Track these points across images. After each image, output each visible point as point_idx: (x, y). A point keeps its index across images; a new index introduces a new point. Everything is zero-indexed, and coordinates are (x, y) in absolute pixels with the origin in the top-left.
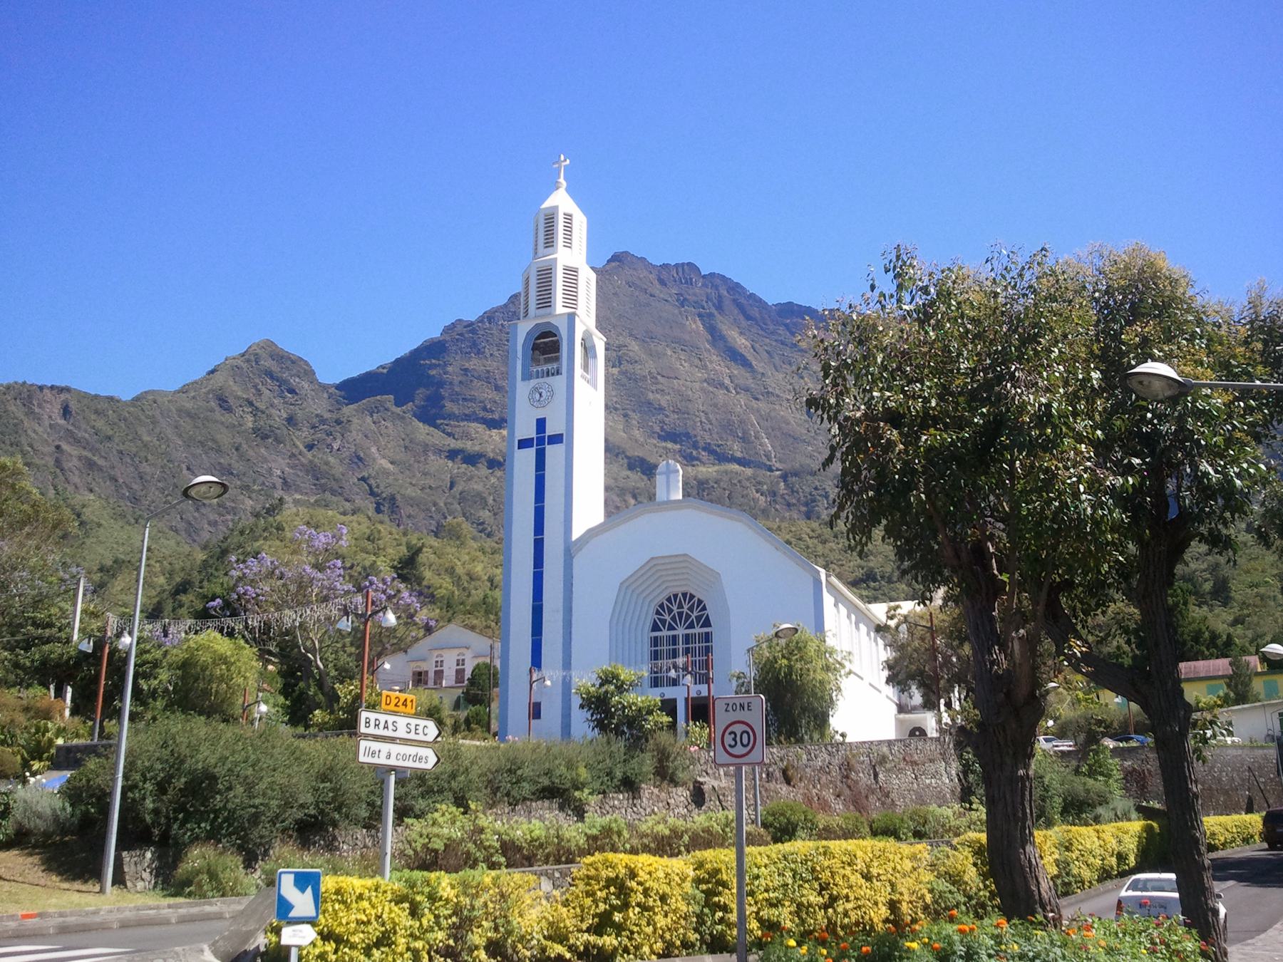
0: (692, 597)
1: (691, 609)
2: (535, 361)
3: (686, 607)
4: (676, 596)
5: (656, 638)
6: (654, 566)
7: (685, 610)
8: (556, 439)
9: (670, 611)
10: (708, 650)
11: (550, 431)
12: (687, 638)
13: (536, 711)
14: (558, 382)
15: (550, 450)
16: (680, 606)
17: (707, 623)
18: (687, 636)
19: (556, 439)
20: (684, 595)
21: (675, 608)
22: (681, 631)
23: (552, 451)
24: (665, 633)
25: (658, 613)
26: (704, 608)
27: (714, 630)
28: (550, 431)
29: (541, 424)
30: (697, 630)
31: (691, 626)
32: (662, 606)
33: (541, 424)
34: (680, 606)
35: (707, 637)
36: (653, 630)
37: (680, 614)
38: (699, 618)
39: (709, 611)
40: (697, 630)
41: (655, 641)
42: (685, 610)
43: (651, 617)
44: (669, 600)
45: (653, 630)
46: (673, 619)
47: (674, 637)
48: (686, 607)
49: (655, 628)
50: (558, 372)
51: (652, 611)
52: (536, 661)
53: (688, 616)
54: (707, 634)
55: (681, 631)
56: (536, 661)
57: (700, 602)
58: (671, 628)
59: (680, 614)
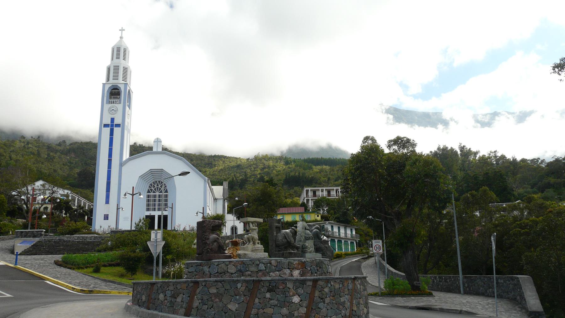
0: (162, 183)
2: (110, 98)
4: (156, 182)
6: (152, 172)
7: (159, 186)
8: (118, 125)
9: (154, 187)
11: (116, 122)
12: (159, 196)
13: (106, 217)
14: (120, 107)
15: (116, 129)
16: (158, 185)
17: (166, 191)
19: (118, 125)
20: (159, 182)
22: (157, 194)
23: (117, 130)
24: (152, 194)
25: (150, 187)
26: (166, 187)
28: (116, 122)
29: (112, 120)
31: (161, 192)
32: (151, 185)
33: (112, 120)
34: (158, 185)
35: (166, 196)
41: (148, 196)
42: (159, 186)
43: (148, 188)
44: (154, 183)
46: (155, 189)
49: (149, 192)
50: (120, 103)
51: (148, 186)
52: (107, 202)
53: (160, 189)
55: (157, 194)
56: (107, 202)
58: (154, 192)
59: (157, 188)
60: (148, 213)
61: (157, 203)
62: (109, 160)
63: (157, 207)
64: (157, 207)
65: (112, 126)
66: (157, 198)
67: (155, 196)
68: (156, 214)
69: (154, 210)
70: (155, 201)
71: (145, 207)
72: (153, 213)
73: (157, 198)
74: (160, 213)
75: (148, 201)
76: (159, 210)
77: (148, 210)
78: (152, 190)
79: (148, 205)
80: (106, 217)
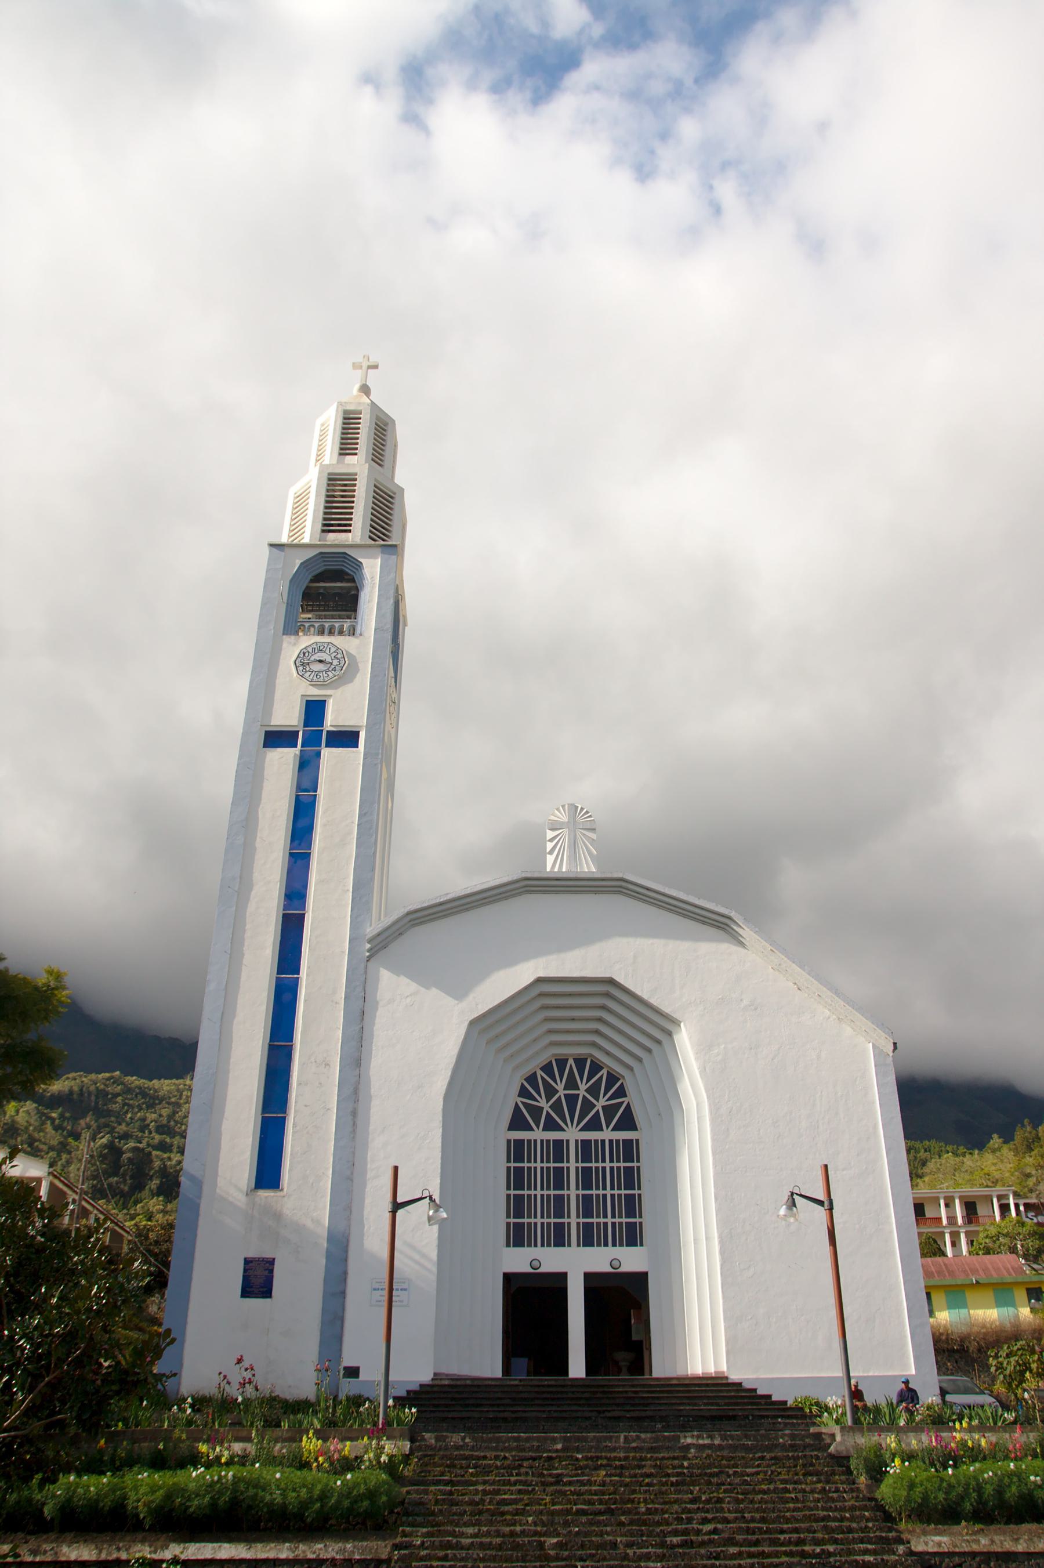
0: (596, 1067)
1: (594, 1090)
3: (583, 1087)
4: (562, 1063)
5: (519, 1143)
8: (346, 738)
9: (551, 1092)
10: (631, 1178)
11: (332, 720)
13: (258, 1280)
15: (328, 755)
16: (571, 1084)
17: (628, 1122)
18: (586, 1144)
20: (580, 1062)
21: (560, 1087)
25: (523, 1092)
26: (621, 1092)
27: (641, 1135)
28: (332, 720)
30: (607, 1134)
31: (594, 1125)
32: (532, 1079)
34: (571, 1084)
35: (630, 1151)
36: (511, 1128)
37: (572, 1100)
38: (610, 1111)
39: (632, 1098)
40: (607, 1134)
41: (517, 1150)
43: (513, 1098)
44: (547, 1068)
45: (511, 1128)
46: (557, 1107)
47: (558, 1143)
48: (583, 1087)
49: (517, 1122)
51: (516, 1089)
52: (268, 1171)
53: (588, 1106)
54: (628, 1143)
55: (572, 1134)
56: (268, 1171)
57: (612, 1078)
58: (551, 1125)
59: (572, 1100)
60: (519, 1260)
61: (573, 1192)
62: (286, 918)
63: (573, 1220)
64: (573, 1220)
65: (313, 740)
66: (572, 1165)
67: (559, 1149)
68: (576, 1263)
69: (559, 1237)
70: (559, 1179)
71: (498, 1220)
72: (551, 1259)
73: (572, 1165)
74: (600, 1259)
75: (517, 1178)
76: (588, 1238)
77: (518, 1237)
78: (536, 1112)
79: (517, 1206)
80: (258, 1280)
